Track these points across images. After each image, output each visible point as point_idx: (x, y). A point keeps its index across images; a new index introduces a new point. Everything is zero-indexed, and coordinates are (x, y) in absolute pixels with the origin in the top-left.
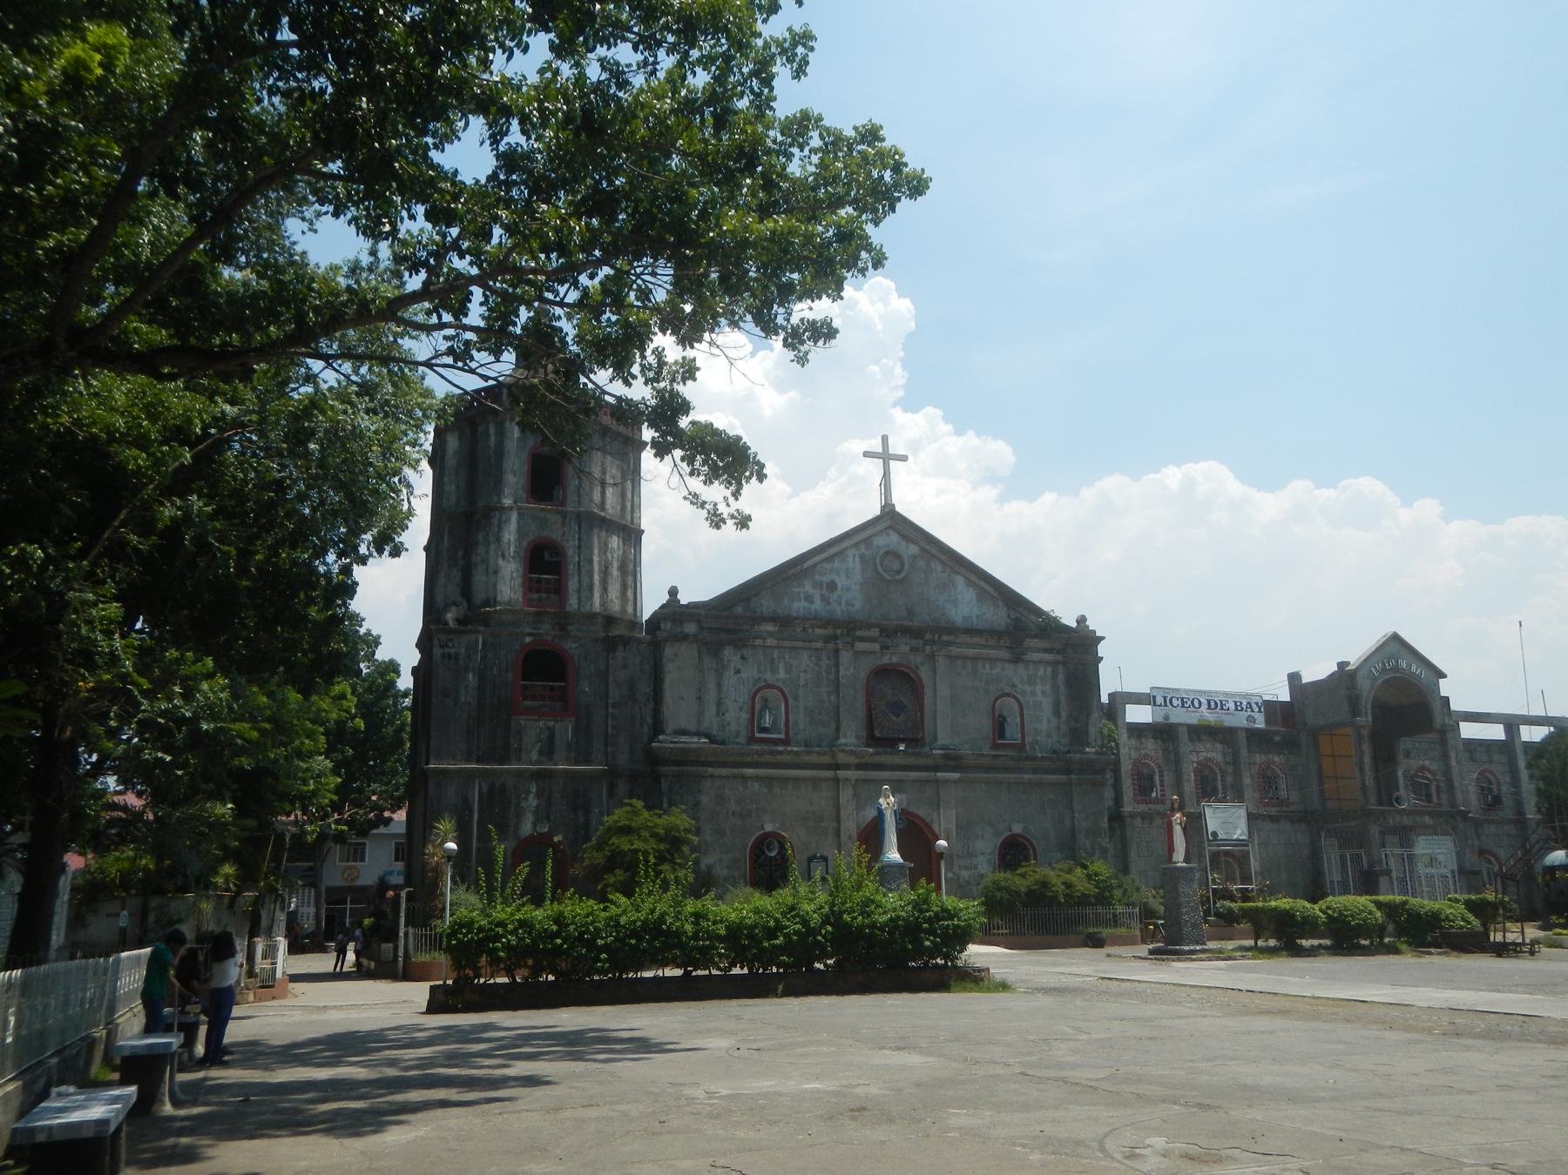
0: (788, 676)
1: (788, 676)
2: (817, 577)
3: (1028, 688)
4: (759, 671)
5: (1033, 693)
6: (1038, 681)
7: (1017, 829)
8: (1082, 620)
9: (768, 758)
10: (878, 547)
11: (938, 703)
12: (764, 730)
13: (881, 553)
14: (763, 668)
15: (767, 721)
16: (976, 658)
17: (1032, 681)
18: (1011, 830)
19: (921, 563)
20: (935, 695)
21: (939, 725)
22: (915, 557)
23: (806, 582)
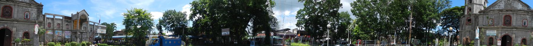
3: (31, 11)
7: (27, 30)
8: (41, 3)
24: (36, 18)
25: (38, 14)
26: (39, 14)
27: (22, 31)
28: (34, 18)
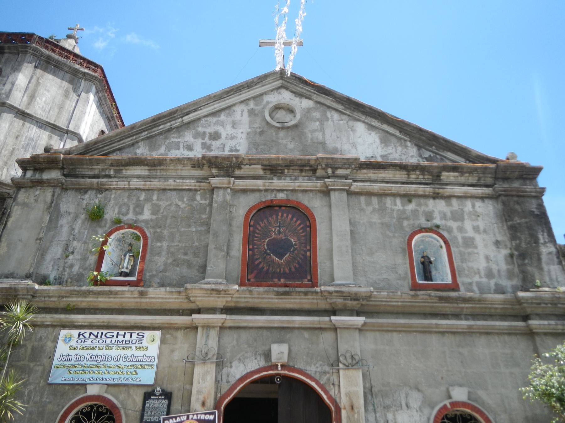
0: (154, 217)
1: (154, 217)
2: (200, 129)
3: (454, 225)
4: (119, 213)
5: (461, 229)
6: (466, 217)
9: (103, 302)
10: (268, 103)
11: (335, 239)
12: (121, 274)
13: (271, 105)
14: (124, 210)
15: (126, 265)
16: (382, 195)
17: (458, 217)
18: (450, 397)
19: (317, 115)
20: (331, 229)
21: (335, 262)
22: (309, 110)
23: (186, 133)
24: (510, 275)
25: (513, 237)
26: (524, 236)
27: (415, 399)
28: (490, 274)
